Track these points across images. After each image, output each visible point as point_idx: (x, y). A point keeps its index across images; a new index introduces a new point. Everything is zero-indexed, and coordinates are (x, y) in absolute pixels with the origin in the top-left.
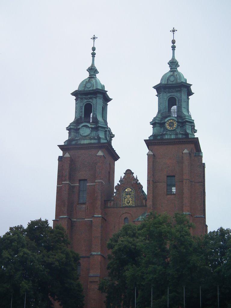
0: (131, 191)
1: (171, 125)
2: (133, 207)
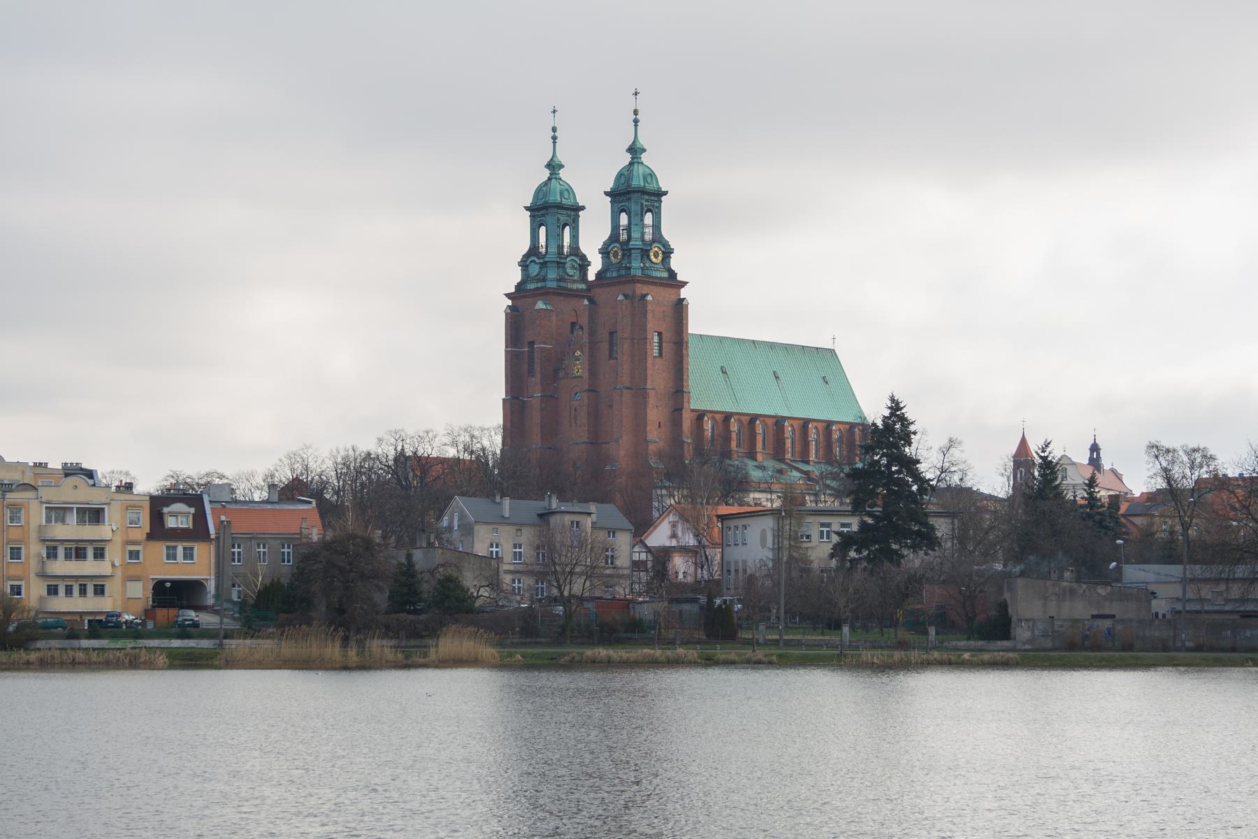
1: (616, 255)
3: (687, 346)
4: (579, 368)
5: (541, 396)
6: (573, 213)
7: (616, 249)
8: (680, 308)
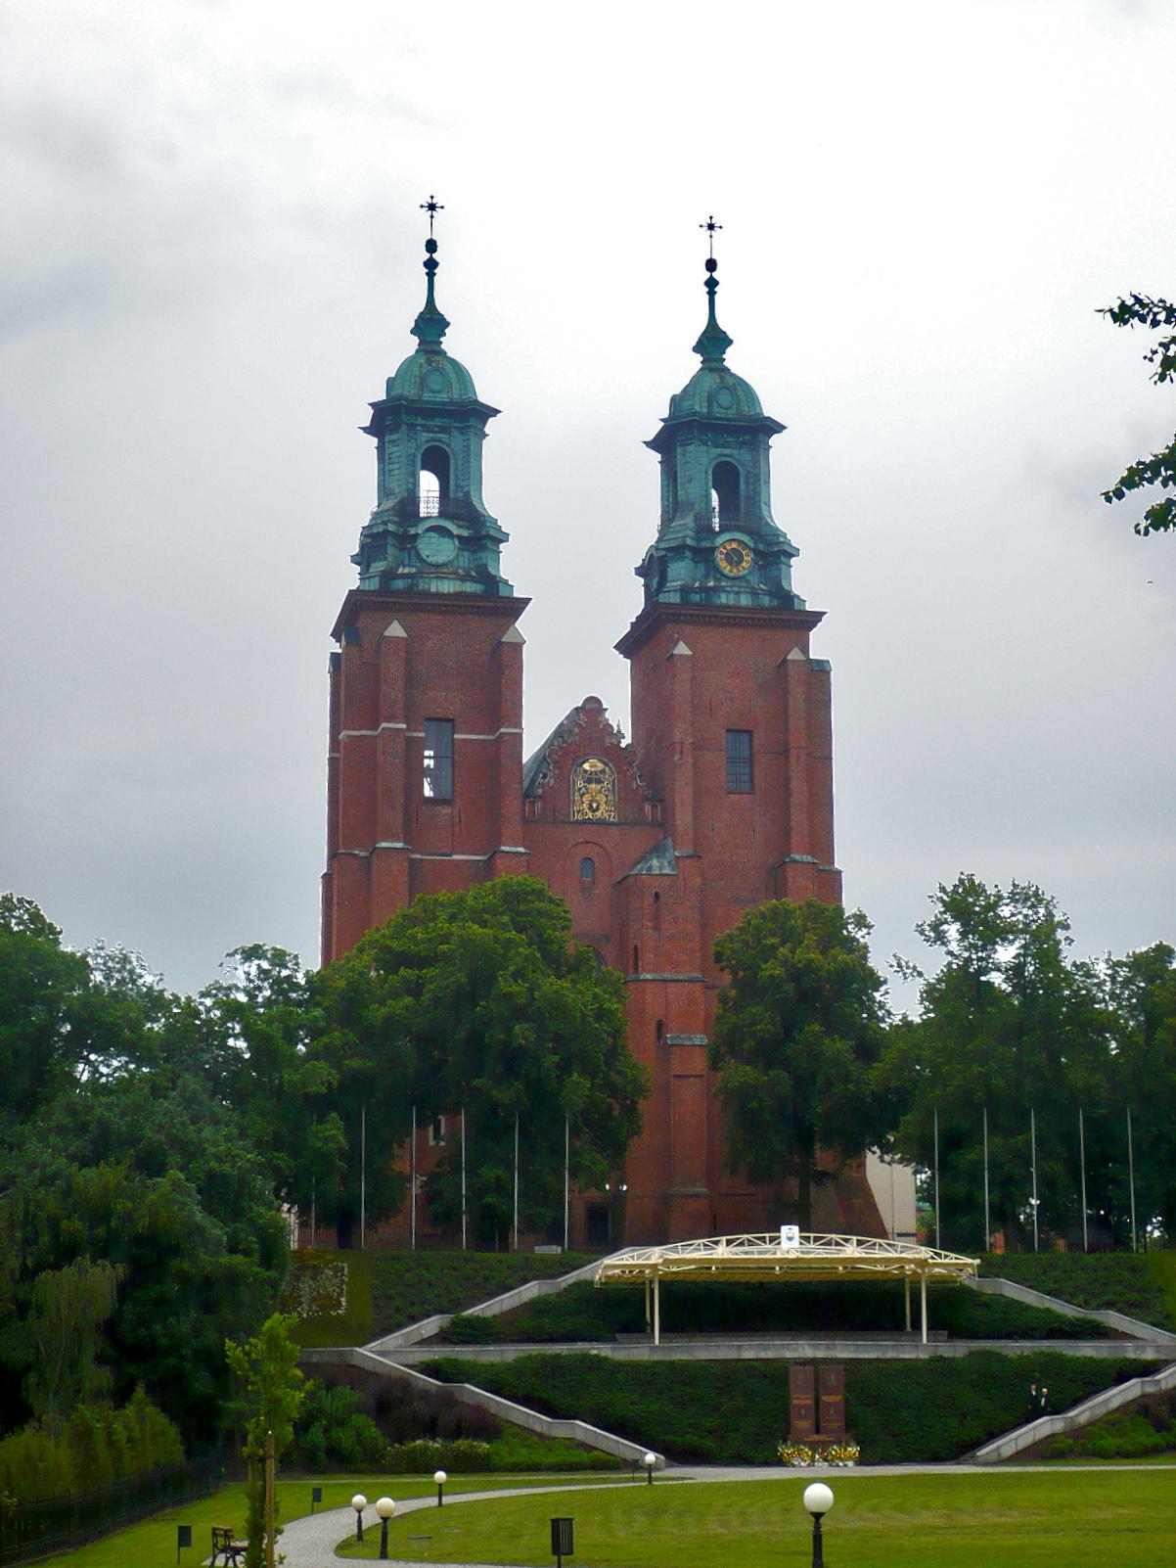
0: (603, 772)
2: (612, 824)
7: (734, 545)
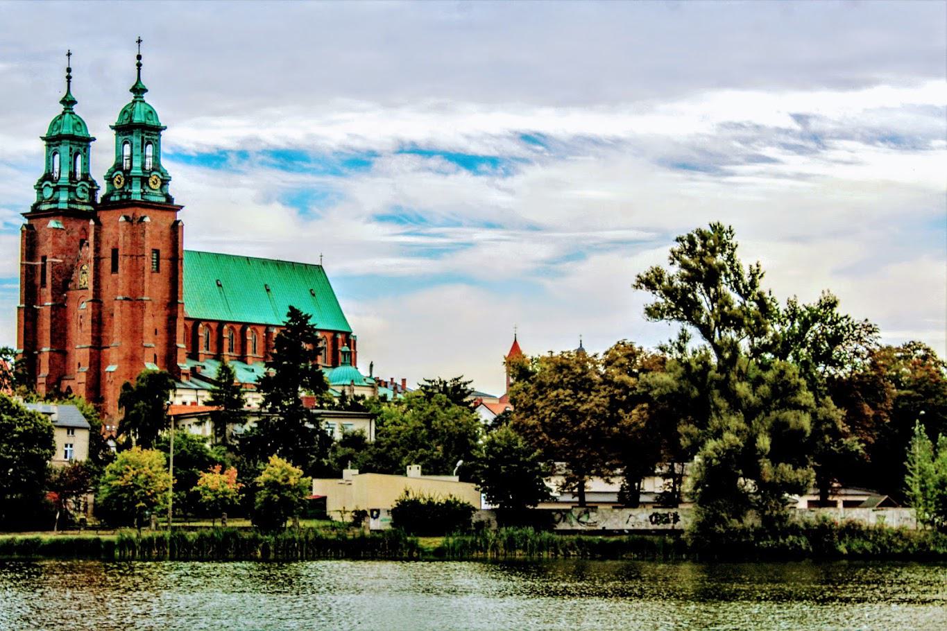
3: (182, 263)
4: (85, 278)
5: (52, 306)
6: (84, 144)
8: (175, 228)
